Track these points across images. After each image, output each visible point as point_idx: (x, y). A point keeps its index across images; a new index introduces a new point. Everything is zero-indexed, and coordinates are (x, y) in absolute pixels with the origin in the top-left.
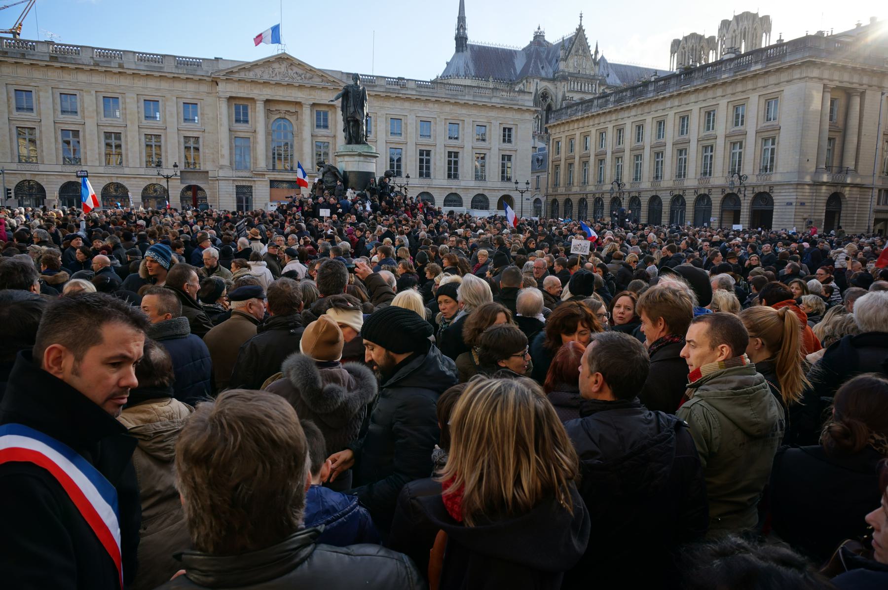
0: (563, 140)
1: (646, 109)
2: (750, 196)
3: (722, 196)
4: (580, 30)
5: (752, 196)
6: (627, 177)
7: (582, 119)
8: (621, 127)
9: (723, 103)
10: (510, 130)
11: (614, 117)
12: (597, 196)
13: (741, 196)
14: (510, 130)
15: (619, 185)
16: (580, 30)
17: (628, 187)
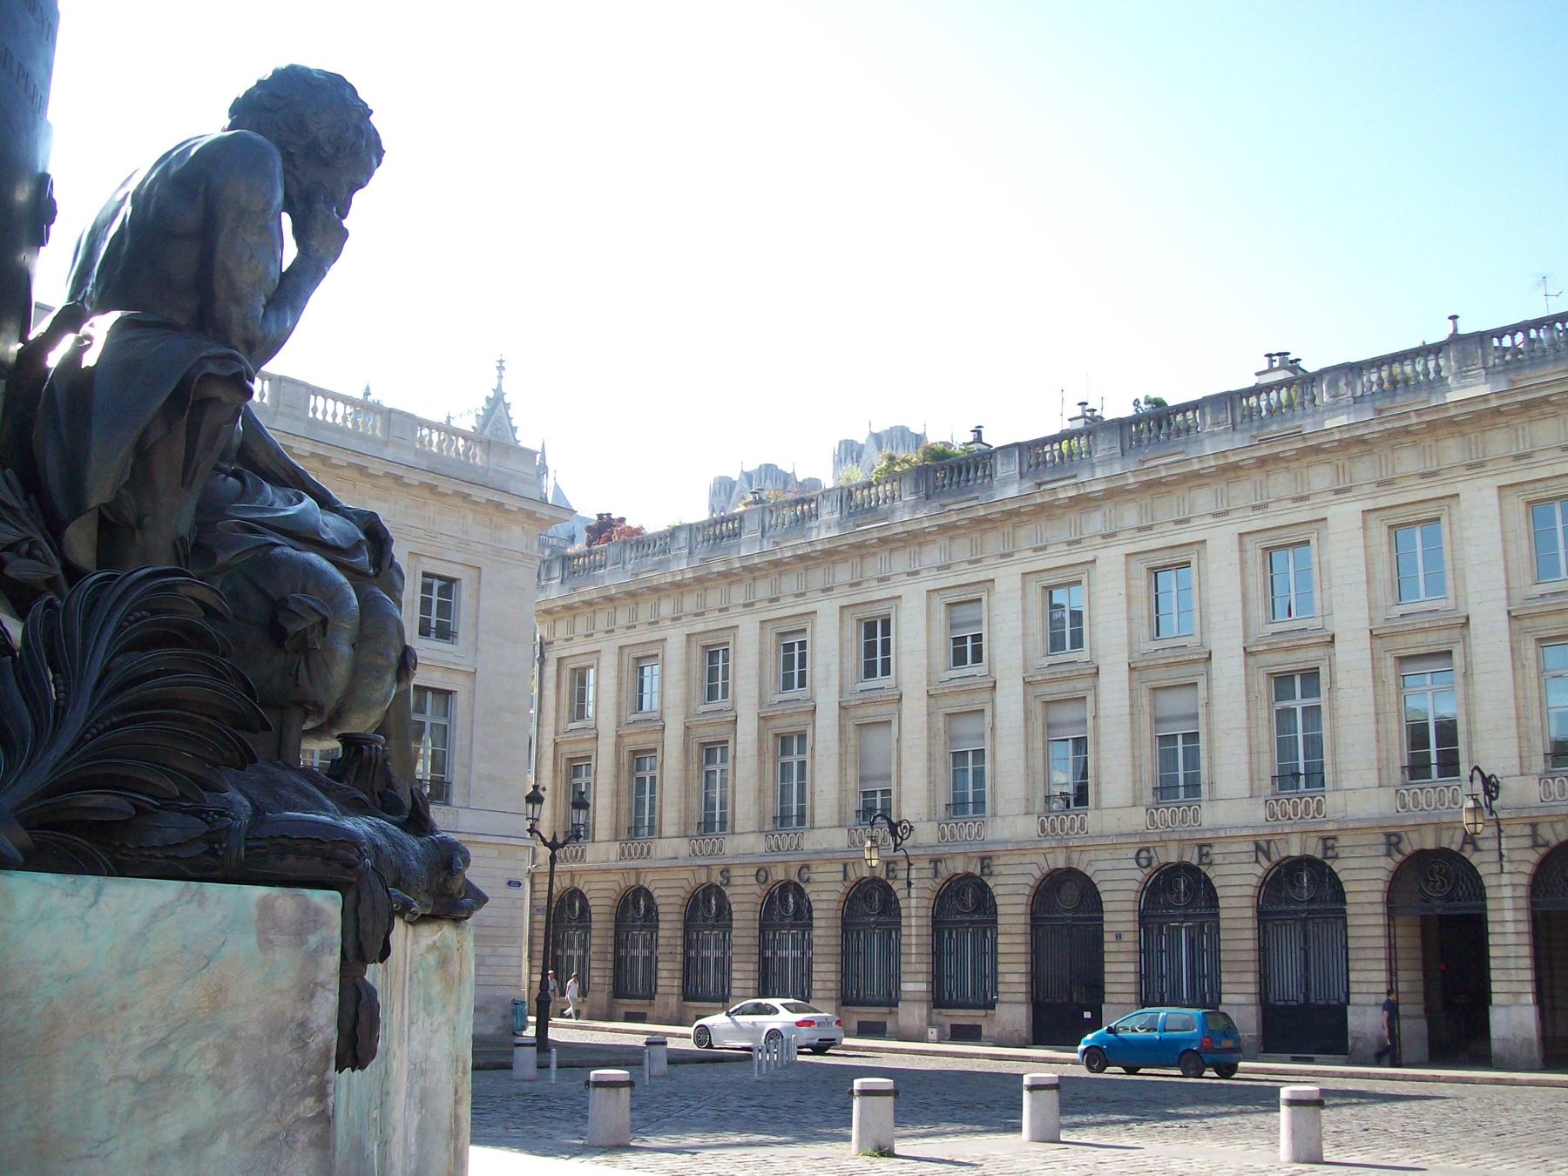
0: (609, 662)
1: (993, 542)
2: (1524, 861)
3: (1390, 864)
4: (497, 404)
5: (1534, 856)
6: (915, 799)
7: (699, 580)
8: (878, 611)
9: (1344, 516)
10: (449, 584)
11: (843, 574)
12: (778, 874)
13: (1484, 863)
14: (449, 584)
15: (893, 828)
16: (497, 404)
17: (925, 834)
